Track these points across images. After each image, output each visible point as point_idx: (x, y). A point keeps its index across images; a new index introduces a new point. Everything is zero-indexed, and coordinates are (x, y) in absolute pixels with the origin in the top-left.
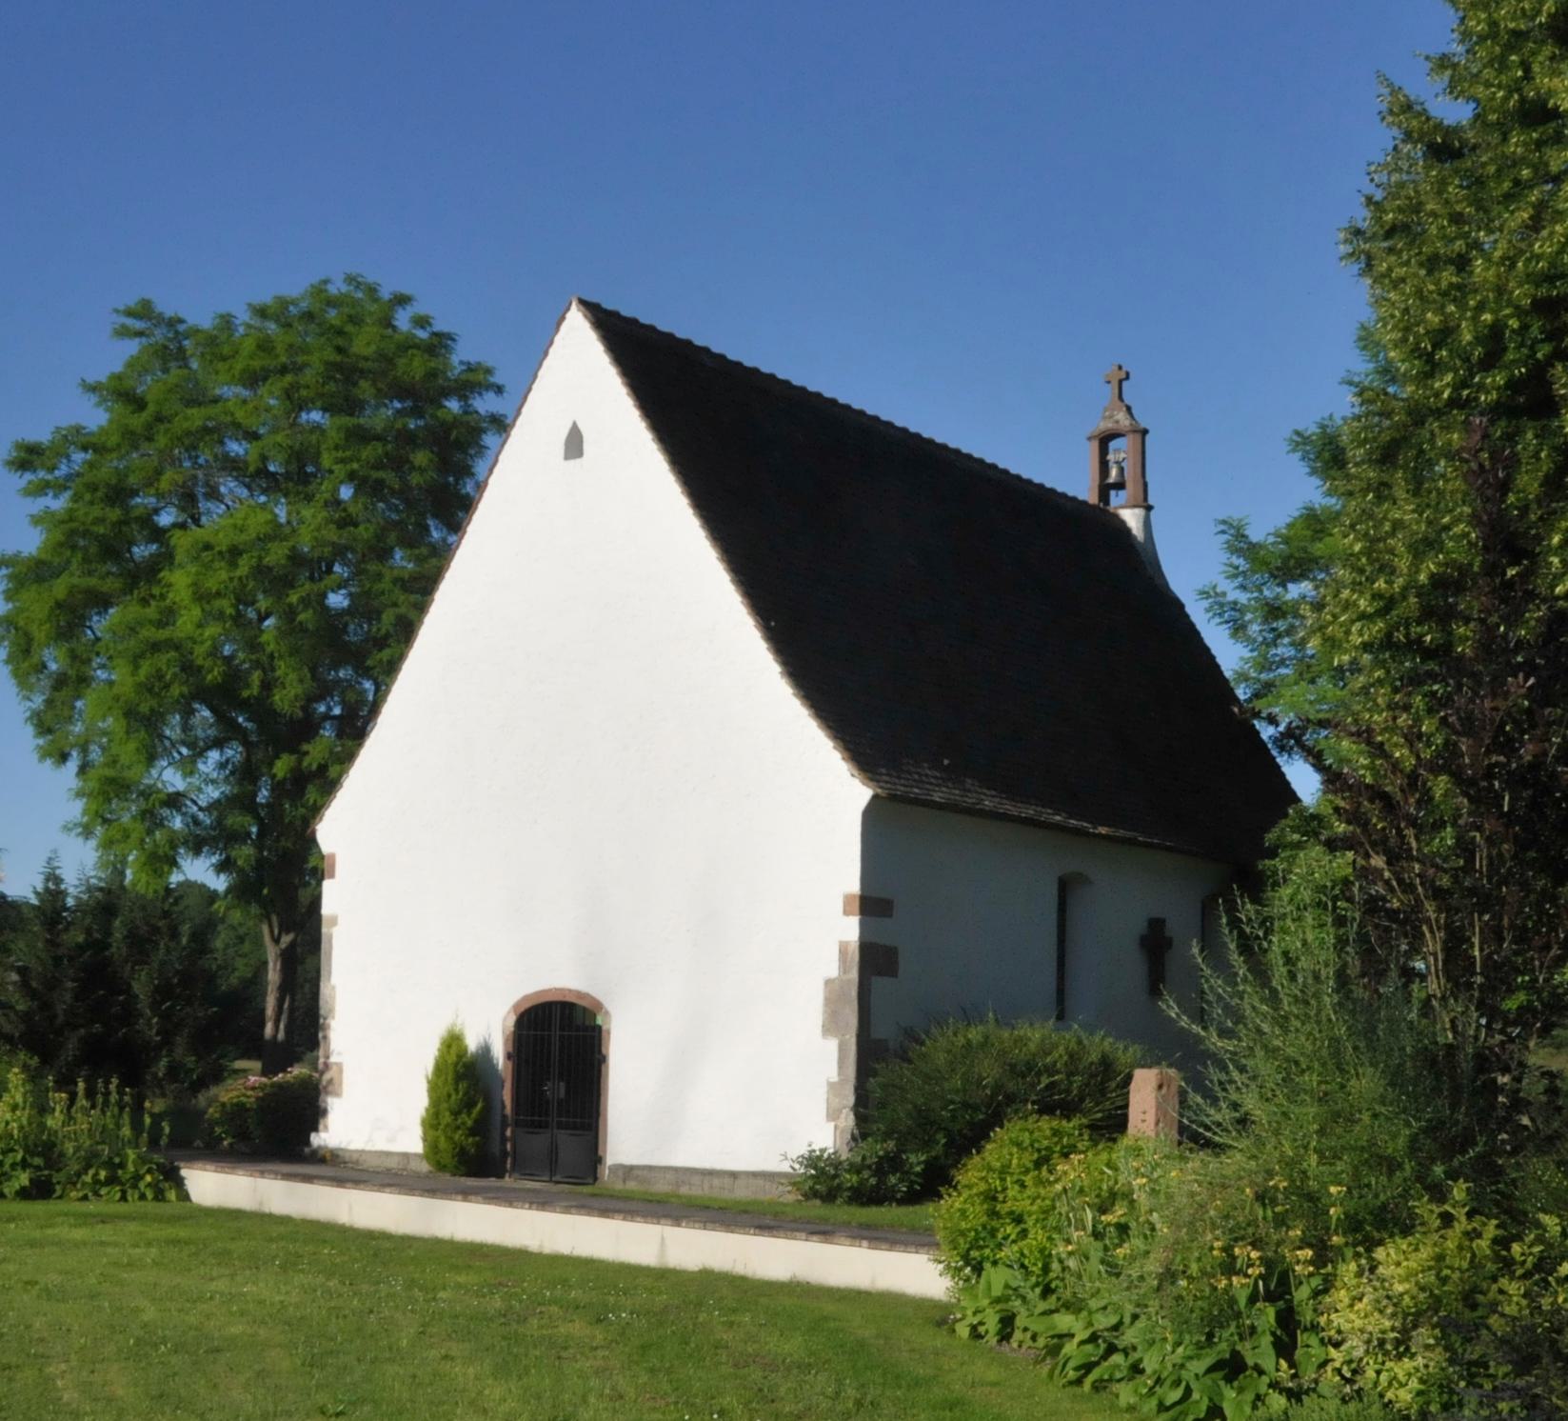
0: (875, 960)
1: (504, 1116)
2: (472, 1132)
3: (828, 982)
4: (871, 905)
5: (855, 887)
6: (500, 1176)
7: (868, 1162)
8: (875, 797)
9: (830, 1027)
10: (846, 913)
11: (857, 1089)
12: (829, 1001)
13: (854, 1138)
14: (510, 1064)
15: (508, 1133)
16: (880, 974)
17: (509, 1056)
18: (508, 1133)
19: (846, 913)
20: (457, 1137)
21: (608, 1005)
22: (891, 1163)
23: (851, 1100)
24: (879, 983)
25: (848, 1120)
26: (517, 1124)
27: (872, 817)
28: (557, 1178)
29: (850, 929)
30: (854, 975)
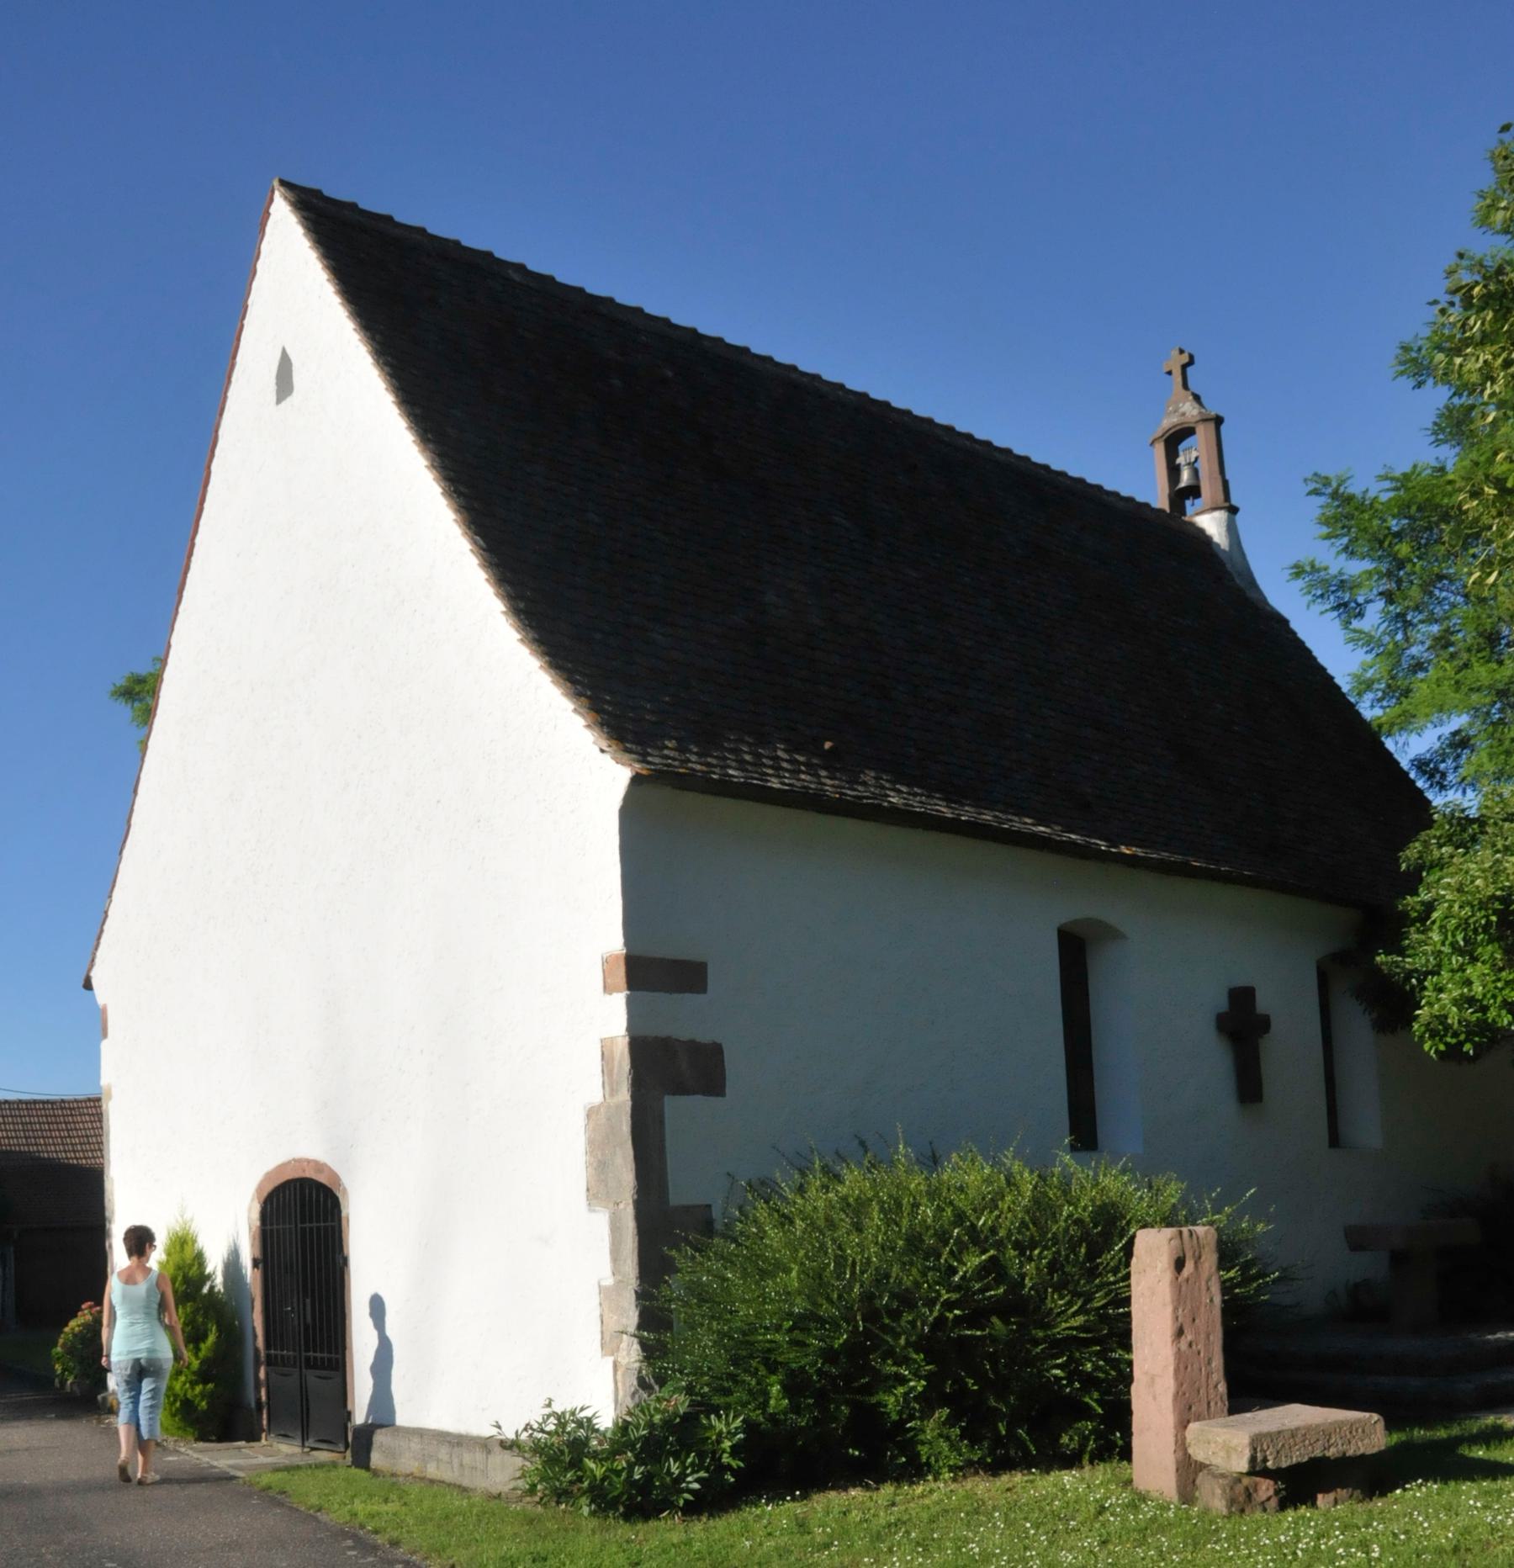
0: (665, 1071)
1: (256, 1350)
2: (203, 1376)
3: (591, 1113)
4: (647, 972)
5: (615, 942)
6: (253, 1437)
7: (634, 1434)
8: (636, 780)
9: (596, 1194)
10: (608, 989)
11: (640, 1296)
12: (593, 1145)
13: (643, 1384)
14: (258, 1273)
15: (262, 1375)
16: (681, 1089)
17: (255, 1263)
18: (262, 1375)
19: (608, 989)
20: (177, 1386)
21: (346, 1180)
22: (680, 1435)
23: (632, 1318)
24: (675, 1108)
25: (631, 1353)
26: (270, 1362)
27: (631, 812)
28: (311, 1442)
29: (611, 1016)
30: (624, 1096)
